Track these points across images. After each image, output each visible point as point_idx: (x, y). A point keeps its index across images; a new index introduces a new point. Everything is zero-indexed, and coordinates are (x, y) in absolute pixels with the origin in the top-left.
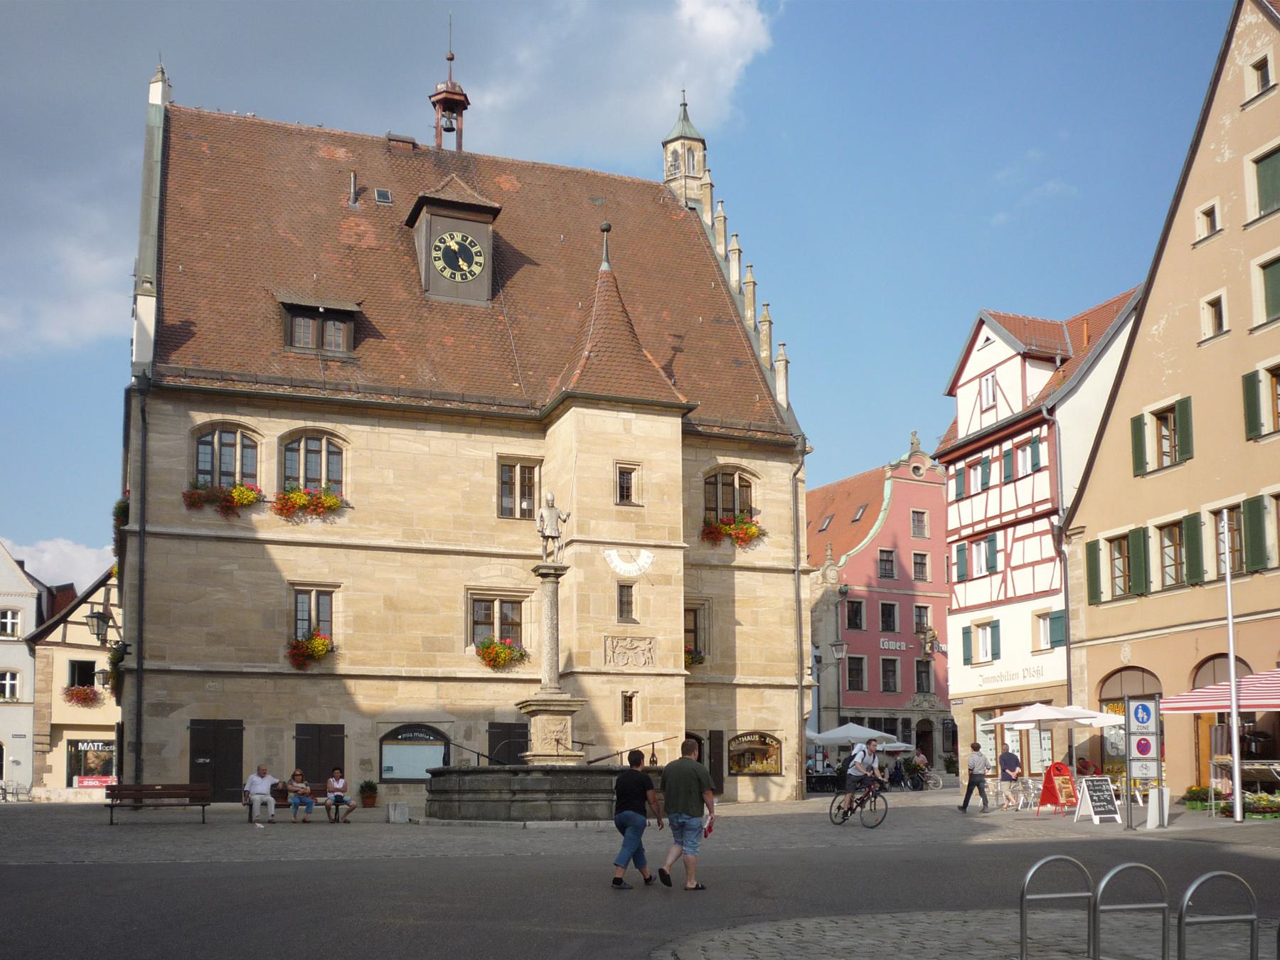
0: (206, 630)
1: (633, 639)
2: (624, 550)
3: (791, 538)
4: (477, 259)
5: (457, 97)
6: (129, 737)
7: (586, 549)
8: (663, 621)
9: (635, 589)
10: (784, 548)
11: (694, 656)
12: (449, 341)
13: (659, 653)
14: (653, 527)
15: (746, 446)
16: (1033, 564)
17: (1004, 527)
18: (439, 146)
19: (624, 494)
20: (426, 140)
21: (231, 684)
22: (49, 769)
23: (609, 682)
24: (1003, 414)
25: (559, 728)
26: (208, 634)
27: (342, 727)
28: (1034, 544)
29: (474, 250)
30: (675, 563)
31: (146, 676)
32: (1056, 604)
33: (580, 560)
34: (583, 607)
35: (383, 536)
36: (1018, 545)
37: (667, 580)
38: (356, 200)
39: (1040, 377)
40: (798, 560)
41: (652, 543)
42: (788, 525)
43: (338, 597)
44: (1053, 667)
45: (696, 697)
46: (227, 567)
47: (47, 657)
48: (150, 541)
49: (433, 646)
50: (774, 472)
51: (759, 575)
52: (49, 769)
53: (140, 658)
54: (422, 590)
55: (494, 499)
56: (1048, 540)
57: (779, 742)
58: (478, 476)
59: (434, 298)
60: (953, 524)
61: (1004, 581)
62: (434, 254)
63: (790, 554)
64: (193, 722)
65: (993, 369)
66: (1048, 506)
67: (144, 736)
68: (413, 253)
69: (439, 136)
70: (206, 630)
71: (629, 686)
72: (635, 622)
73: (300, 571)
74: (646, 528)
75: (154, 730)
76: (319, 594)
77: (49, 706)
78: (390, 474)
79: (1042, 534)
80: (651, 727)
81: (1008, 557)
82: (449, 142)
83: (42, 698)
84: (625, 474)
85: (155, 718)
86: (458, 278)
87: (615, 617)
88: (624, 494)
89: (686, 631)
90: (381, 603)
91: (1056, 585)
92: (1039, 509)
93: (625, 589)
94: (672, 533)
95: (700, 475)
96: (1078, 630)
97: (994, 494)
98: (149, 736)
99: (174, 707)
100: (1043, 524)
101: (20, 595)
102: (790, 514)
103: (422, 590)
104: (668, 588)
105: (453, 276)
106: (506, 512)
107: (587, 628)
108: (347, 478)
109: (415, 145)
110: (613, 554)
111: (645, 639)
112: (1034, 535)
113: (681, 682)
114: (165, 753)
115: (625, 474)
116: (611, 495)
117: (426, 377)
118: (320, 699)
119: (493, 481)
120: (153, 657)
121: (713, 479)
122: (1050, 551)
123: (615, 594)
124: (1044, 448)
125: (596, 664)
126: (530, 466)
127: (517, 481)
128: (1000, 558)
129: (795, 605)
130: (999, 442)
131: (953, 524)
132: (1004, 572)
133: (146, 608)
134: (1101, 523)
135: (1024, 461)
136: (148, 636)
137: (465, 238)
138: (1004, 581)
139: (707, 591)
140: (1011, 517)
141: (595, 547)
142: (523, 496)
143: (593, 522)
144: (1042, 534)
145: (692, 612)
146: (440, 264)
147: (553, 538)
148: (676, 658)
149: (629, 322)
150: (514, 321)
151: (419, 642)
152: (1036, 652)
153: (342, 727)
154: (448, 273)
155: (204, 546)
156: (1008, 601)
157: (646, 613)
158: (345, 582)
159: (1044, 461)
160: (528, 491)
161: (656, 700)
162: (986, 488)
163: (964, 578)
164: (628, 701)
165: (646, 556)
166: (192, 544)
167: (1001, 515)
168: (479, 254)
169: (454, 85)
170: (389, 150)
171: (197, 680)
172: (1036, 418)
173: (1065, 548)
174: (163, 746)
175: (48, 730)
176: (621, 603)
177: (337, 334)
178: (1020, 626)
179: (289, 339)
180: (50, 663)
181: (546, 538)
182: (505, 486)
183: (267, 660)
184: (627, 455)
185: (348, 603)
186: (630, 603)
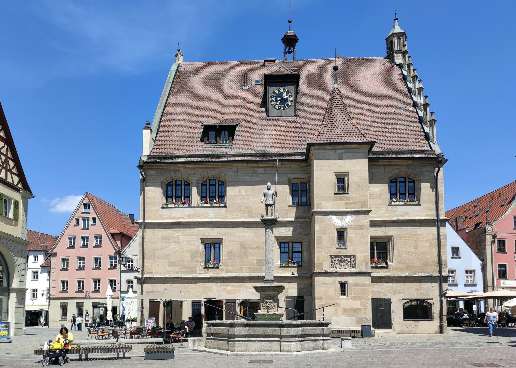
0: (168, 260)
1: (345, 256)
14: (354, 203)
26: (169, 262)
29: (277, 93)
37: (361, 227)
46: (177, 235)
53: (143, 274)
54: (256, 240)
71: (343, 279)
95: (387, 178)
107: (321, 252)
110: (334, 217)
120: (148, 273)
121: (394, 180)
125: (327, 267)
136: (145, 264)
143: (323, 203)
148: (366, 264)
151: (255, 262)
165: (349, 218)
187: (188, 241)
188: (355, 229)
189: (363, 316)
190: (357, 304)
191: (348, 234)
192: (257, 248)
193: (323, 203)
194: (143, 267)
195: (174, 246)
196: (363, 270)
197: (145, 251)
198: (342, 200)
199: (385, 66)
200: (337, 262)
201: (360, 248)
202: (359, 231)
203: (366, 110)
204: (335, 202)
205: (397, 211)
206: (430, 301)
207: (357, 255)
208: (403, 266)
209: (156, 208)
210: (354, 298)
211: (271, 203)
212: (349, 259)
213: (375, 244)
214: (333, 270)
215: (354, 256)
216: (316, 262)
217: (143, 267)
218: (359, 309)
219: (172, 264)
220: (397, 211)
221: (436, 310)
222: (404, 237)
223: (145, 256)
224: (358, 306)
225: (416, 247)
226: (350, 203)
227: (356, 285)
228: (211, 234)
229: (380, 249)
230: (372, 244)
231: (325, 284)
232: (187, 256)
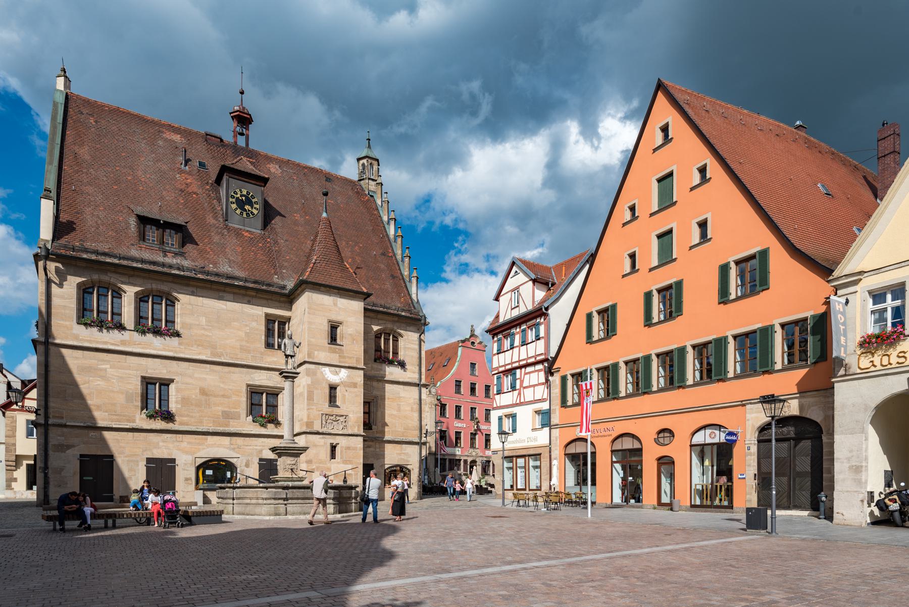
2: (333, 369)
4: (255, 206)
6: (40, 464)
7: (313, 366)
8: (352, 406)
9: (338, 388)
11: (367, 425)
13: (350, 424)
16: (534, 386)
17: (520, 367)
18: (236, 142)
19: (333, 339)
22: (15, 480)
24: (522, 310)
25: (293, 462)
28: (536, 376)
30: (359, 377)
31: (51, 428)
32: (545, 406)
33: (308, 373)
34: (310, 397)
35: (199, 354)
37: (355, 385)
38: (186, 165)
39: (540, 294)
40: (420, 379)
41: (347, 365)
42: (416, 361)
43: (172, 387)
44: (542, 437)
45: (369, 447)
47: (13, 417)
49: (227, 415)
52: (15, 480)
53: (47, 417)
54: (222, 385)
55: (263, 337)
56: (542, 374)
57: (409, 471)
58: (254, 324)
59: (230, 225)
60: (495, 365)
61: (519, 394)
62: (231, 200)
63: (417, 376)
64: (81, 456)
65: (518, 288)
66: (543, 357)
67: (49, 463)
68: (219, 200)
72: (338, 407)
75: (55, 460)
76: (161, 385)
77: (14, 445)
79: (539, 371)
80: (345, 462)
81: (522, 382)
83: (11, 441)
84: (334, 328)
86: (245, 215)
87: (327, 404)
88: (333, 339)
89: (364, 413)
90: (198, 391)
91: (545, 396)
92: (538, 358)
93: (333, 388)
94: (358, 361)
96: (555, 420)
97: (516, 350)
98: (53, 462)
99: (69, 447)
100: (540, 367)
104: (356, 390)
105: (241, 214)
106: (269, 345)
108: (178, 320)
110: (326, 370)
112: (536, 371)
114: (63, 474)
115: (334, 328)
116: (324, 339)
117: (225, 268)
119: (263, 328)
120: (54, 417)
122: (543, 380)
123: (327, 391)
124: (542, 328)
126: (284, 322)
127: (276, 330)
128: (518, 382)
129: (418, 401)
130: (520, 325)
131: (495, 365)
132: (520, 390)
135: (531, 335)
137: (248, 193)
138: (519, 394)
139: (375, 393)
140: (524, 362)
142: (279, 337)
144: (539, 371)
145: (367, 403)
146: (234, 206)
147: (292, 356)
148: (359, 426)
149: (337, 246)
150: (276, 242)
152: (534, 430)
154: (238, 211)
156: (521, 404)
157: (344, 402)
158: (177, 379)
160: (282, 335)
161: (348, 448)
162: (512, 348)
163: (499, 392)
165: (344, 373)
167: (519, 361)
168: (256, 203)
169: (244, 108)
172: (539, 313)
173: (550, 378)
174: (62, 469)
175: (14, 458)
176: (331, 397)
177: (173, 240)
178: (526, 417)
180: (14, 421)
181: (287, 356)
182: (269, 332)
183: (129, 421)
184: (336, 317)
185: (178, 390)
186: (335, 397)
187: (121, 377)
192: (223, 396)
197: (51, 385)
198: (335, 352)
202: (352, 390)
211: (292, 354)
226: (344, 357)
228: (157, 371)
232: (121, 399)
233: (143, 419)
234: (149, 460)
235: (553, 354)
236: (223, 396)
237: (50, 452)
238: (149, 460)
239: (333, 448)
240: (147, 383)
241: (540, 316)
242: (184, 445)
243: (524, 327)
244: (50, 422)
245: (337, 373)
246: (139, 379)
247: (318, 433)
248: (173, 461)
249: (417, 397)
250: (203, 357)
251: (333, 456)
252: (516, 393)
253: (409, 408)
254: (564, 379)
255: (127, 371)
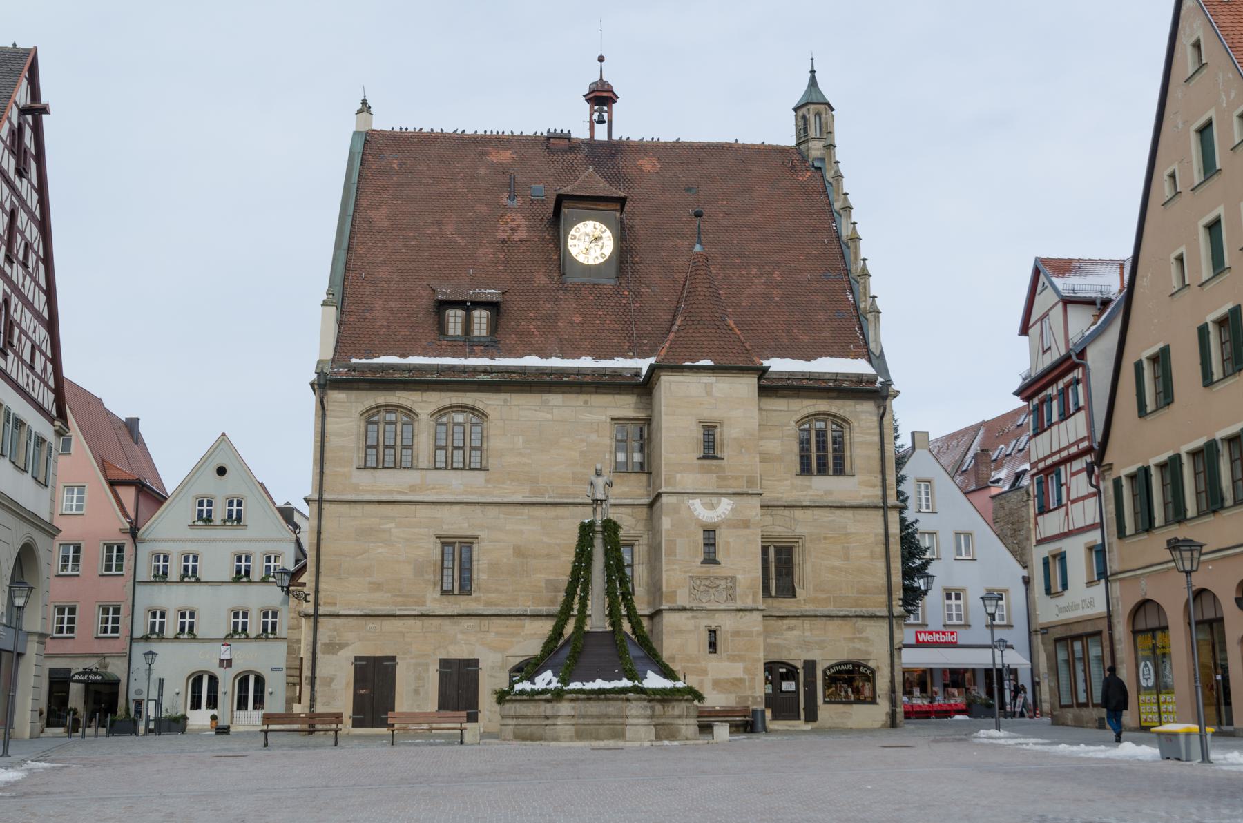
0: (368, 579)
1: (717, 578)
2: (707, 499)
3: (880, 477)
5: (605, 94)
10: (874, 486)
12: (578, 319)
15: (835, 394)
20: (580, 132)
21: (388, 625)
23: (693, 617)
27: (477, 660)
31: (321, 620)
32: (1095, 537)
36: (1074, 479)
37: (746, 524)
40: (884, 497)
41: (730, 491)
46: (387, 526)
48: (325, 506)
50: (863, 417)
51: (849, 513)
53: (316, 604)
54: (546, 539)
58: (594, 437)
63: (879, 492)
64: (357, 658)
69: (592, 129)
70: (368, 579)
73: (445, 527)
74: (725, 478)
78: (519, 441)
82: (601, 134)
85: (327, 656)
90: (511, 551)
99: (342, 646)
101: (281, 540)
102: (877, 454)
103: (546, 539)
109: (570, 139)
110: (697, 505)
111: (726, 578)
113: (757, 616)
114: (333, 686)
118: (459, 636)
125: (682, 599)
129: (882, 538)
132: (1066, 505)
133: (322, 564)
134: (1123, 464)
136: (322, 586)
141: (680, 498)
143: (678, 476)
148: (755, 594)
150: (638, 294)
153: (477, 660)
155: (368, 507)
159: (1082, 403)
162: (1051, 425)
163: (1043, 510)
164: (713, 633)
165: (725, 506)
166: (359, 507)
170: (548, 148)
171: (361, 621)
174: (332, 680)
179: (442, 327)
183: (417, 603)
188: (734, 527)
189: (749, 693)
190: (737, 670)
191: (723, 538)
192: (548, 556)
193: (678, 476)
194: (317, 591)
195: (381, 550)
196: (749, 603)
198: (710, 472)
199: (793, 167)
200: (702, 588)
201: (743, 563)
203: (754, 271)
204: (699, 476)
205: (810, 487)
206: (872, 664)
207: (739, 576)
208: (824, 596)
209: (346, 470)
210: (732, 658)
212: (723, 583)
213: (772, 552)
214: (694, 604)
215: (733, 578)
216: (664, 589)
217: (317, 591)
218: (741, 680)
219: (377, 587)
220: (810, 487)
221: (882, 683)
222: (825, 538)
223: (322, 569)
224: (740, 675)
225: (847, 558)
227: (737, 633)
229: (780, 567)
230: (765, 550)
231: (680, 631)
233: (435, 600)
234: (444, 663)
235: (1099, 436)
236: (548, 556)
237: (319, 655)
238: (444, 663)
239: (713, 633)
240: (444, 544)
241: (1075, 366)
242: (491, 637)
243: (1061, 385)
244: (320, 612)
245: (712, 507)
246: (433, 539)
247: (684, 609)
248: (475, 662)
249: (882, 531)
250: (520, 499)
251: (713, 646)
252: (1063, 510)
253: (866, 553)
254: (1117, 483)
255: (416, 530)
